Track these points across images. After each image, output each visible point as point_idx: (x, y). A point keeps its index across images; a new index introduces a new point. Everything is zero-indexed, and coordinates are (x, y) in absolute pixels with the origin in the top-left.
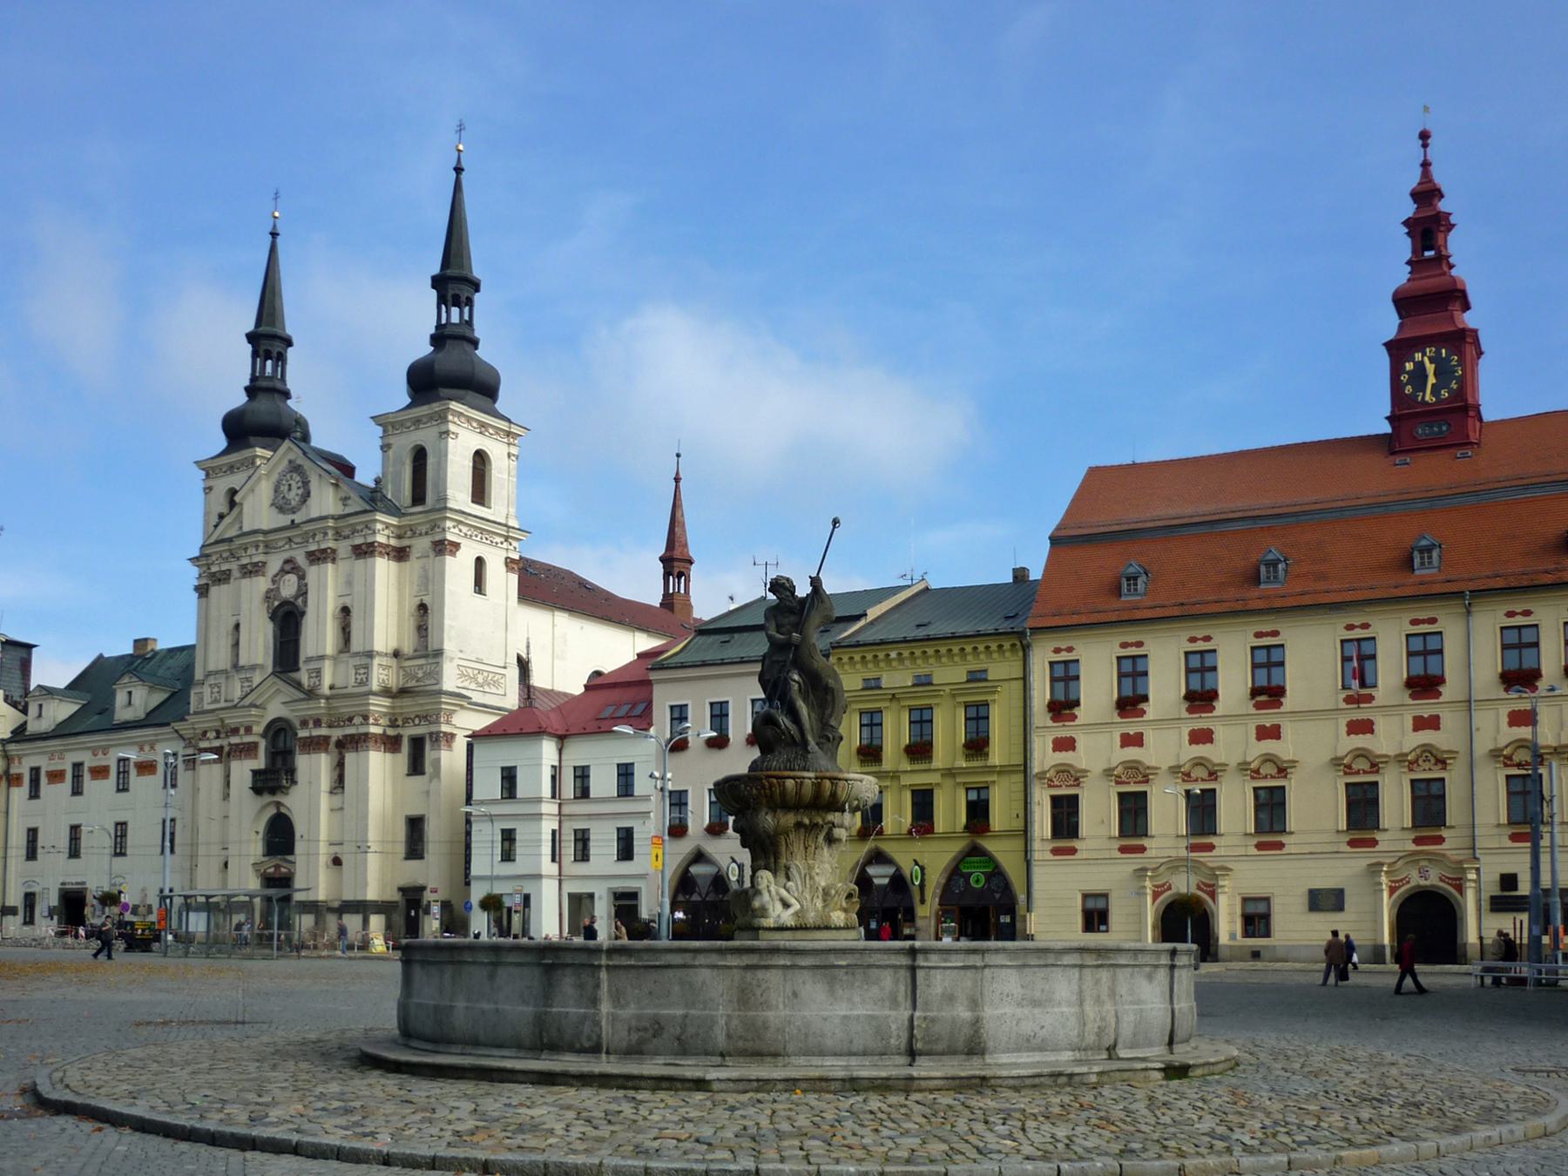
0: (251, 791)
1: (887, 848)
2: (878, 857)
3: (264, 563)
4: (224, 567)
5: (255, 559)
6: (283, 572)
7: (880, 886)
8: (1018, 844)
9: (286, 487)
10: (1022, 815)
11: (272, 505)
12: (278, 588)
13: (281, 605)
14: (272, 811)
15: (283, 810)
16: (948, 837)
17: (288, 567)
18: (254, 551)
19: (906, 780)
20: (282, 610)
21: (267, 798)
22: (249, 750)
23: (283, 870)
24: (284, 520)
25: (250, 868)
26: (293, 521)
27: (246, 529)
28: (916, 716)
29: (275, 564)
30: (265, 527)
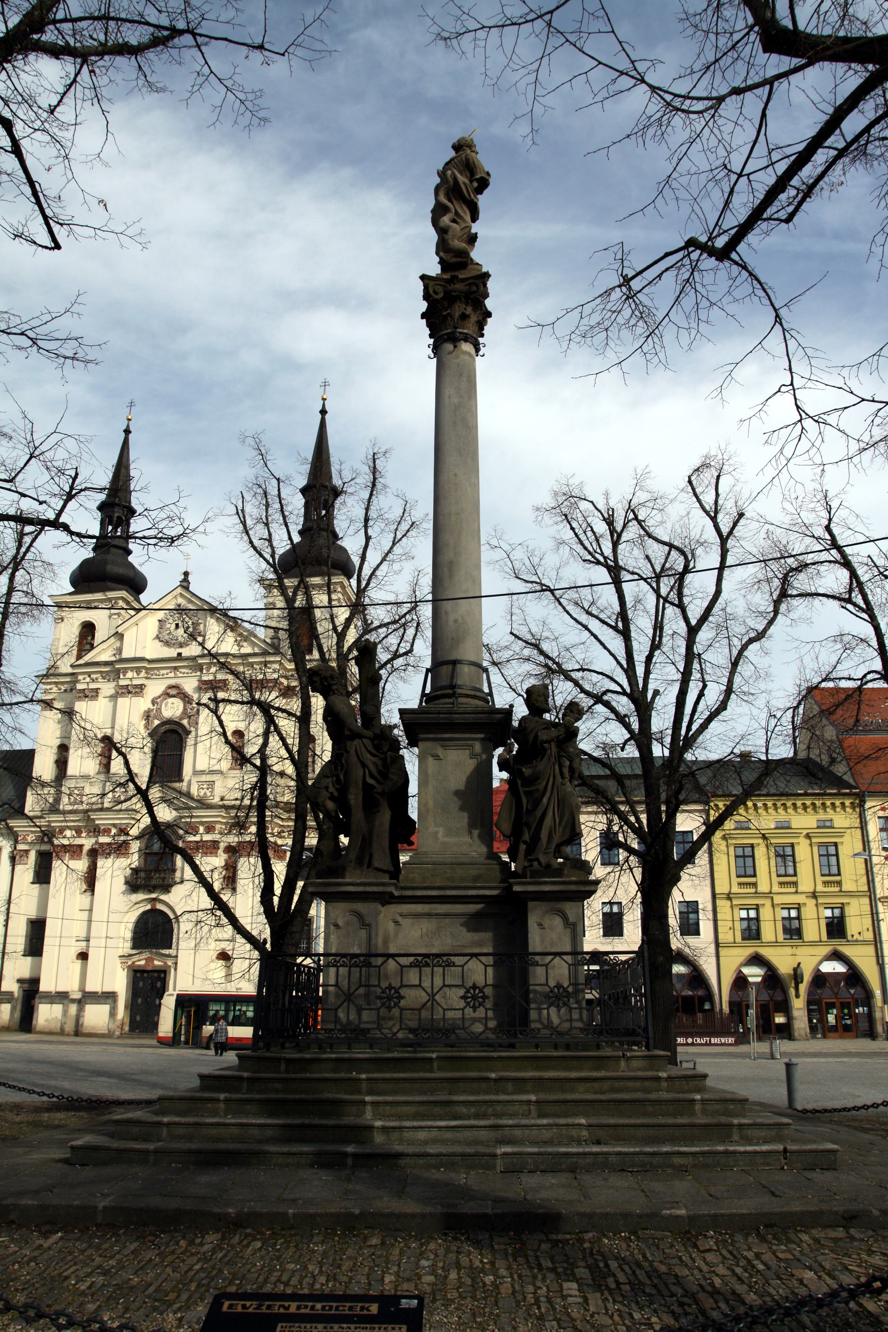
0: (124, 887)
1: (767, 952)
2: (756, 960)
3: (141, 687)
4: (93, 686)
5: (135, 682)
6: (167, 695)
7: (755, 983)
8: (871, 950)
9: (173, 626)
10: (871, 929)
11: (158, 637)
12: (160, 709)
13: (163, 723)
14: (149, 907)
15: (160, 906)
16: (813, 944)
17: (173, 692)
18: (135, 675)
19: (778, 900)
20: (163, 729)
21: (141, 896)
22: (120, 849)
23: (156, 963)
24: (172, 653)
25: (118, 961)
26: (179, 654)
27: (125, 655)
28: (740, 852)
29: (154, 688)
30: (148, 656)
